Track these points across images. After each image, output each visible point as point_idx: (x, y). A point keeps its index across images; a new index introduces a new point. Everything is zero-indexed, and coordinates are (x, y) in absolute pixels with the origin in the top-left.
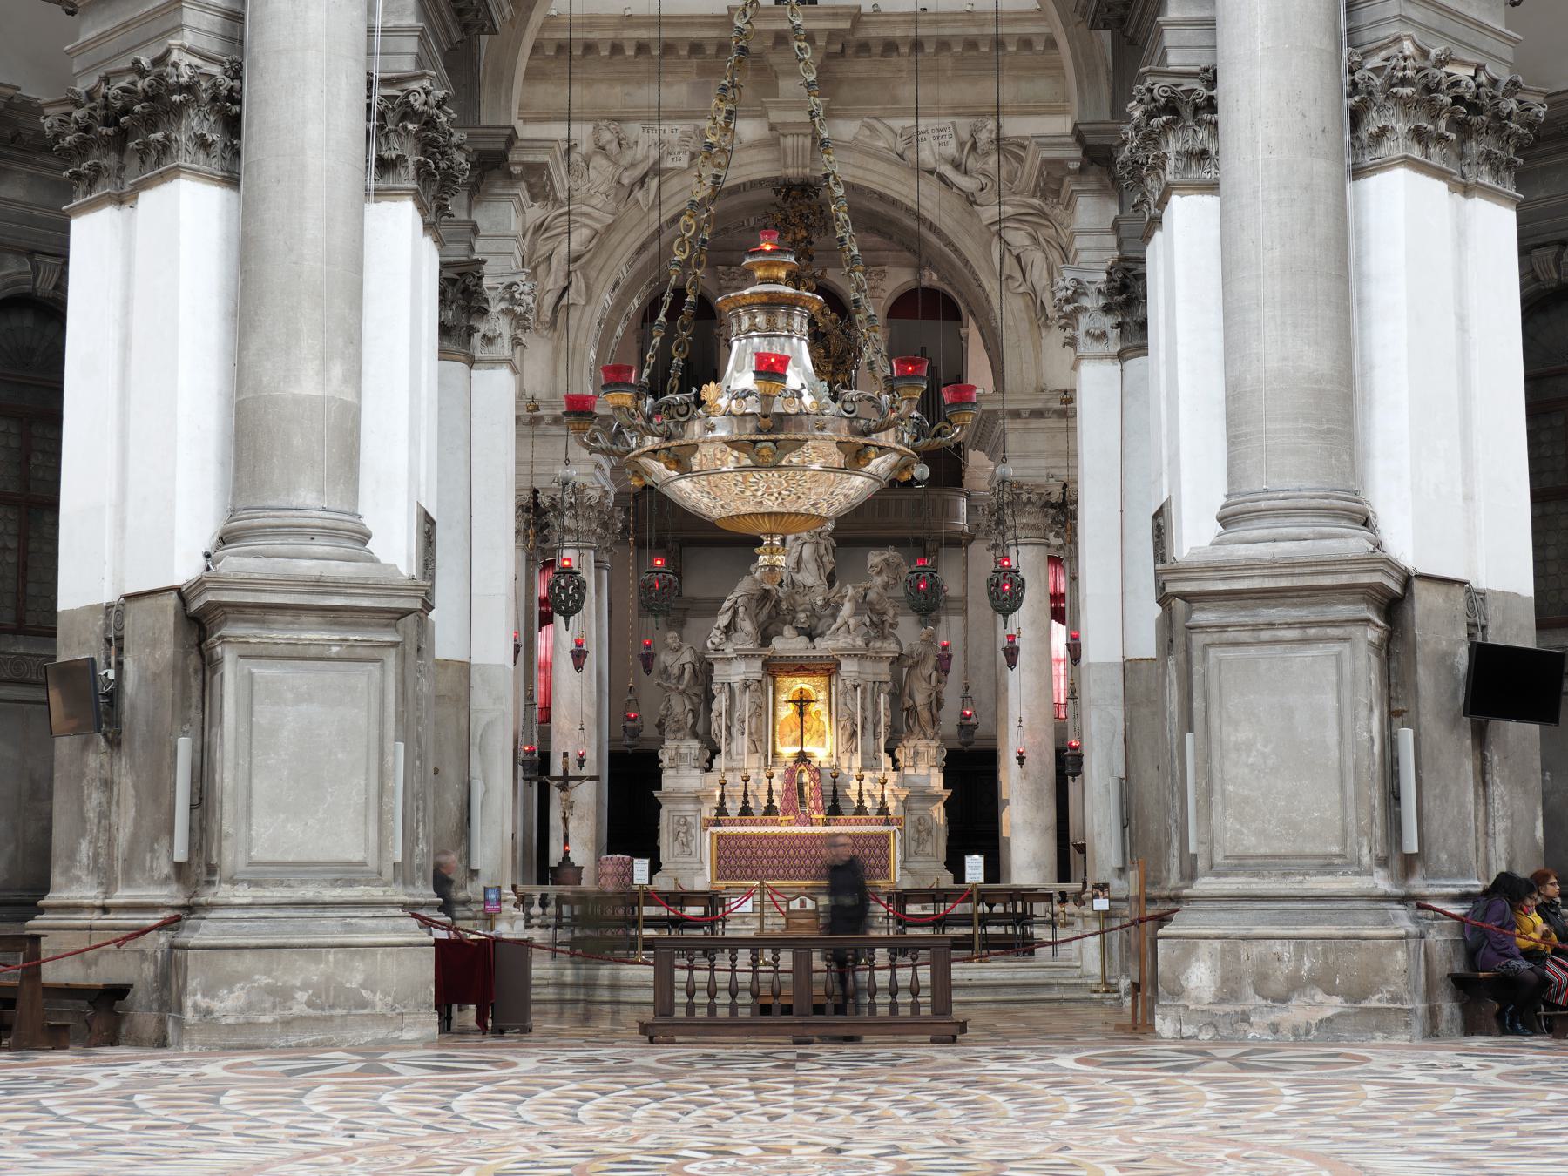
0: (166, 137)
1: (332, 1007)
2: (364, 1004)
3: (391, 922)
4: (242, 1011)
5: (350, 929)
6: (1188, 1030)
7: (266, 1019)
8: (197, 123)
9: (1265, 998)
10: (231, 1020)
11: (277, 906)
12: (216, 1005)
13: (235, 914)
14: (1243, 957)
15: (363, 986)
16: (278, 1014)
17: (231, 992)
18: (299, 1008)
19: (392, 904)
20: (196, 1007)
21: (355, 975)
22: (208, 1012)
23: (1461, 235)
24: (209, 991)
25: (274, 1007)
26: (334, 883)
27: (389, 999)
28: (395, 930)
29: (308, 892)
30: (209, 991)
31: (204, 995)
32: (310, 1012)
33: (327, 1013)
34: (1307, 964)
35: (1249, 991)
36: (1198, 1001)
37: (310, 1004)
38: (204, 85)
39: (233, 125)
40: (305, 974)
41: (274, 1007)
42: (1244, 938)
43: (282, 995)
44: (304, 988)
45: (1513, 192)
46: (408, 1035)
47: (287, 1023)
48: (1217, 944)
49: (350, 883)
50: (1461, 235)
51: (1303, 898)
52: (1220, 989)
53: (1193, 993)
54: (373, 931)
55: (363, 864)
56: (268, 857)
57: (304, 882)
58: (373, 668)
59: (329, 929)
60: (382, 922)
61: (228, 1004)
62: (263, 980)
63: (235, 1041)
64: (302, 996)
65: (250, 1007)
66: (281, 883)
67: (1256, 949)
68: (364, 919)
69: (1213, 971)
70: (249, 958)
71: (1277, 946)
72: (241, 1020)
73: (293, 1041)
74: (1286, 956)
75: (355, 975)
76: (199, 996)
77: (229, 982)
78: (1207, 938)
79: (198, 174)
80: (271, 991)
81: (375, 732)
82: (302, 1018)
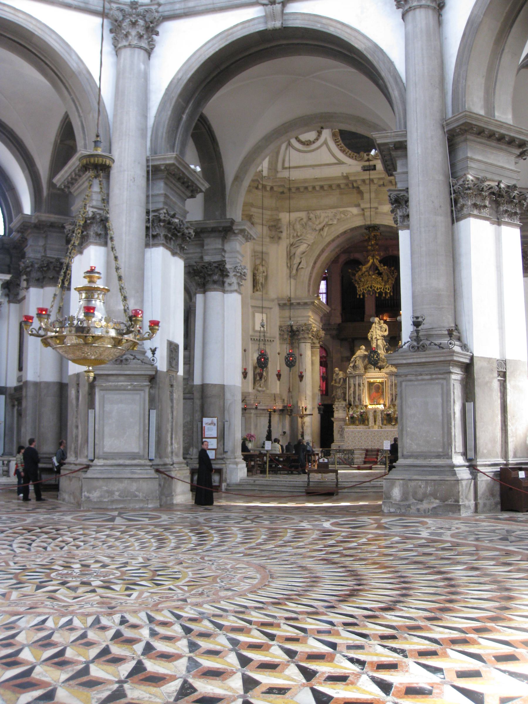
0: (87, 233)
1: (127, 497)
2: (136, 496)
3: (146, 471)
4: (99, 498)
5: (133, 473)
6: (392, 510)
7: (105, 500)
8: (95, 229)
9: (416, 500)
10: (95, 500)
11: (112, 466)
12: (91, 495)
13: (98, 468)
14: (409, 486)
15: (136, 491)
16: (109, 498)
17: (95, 492)
18: (116, 495)
19: (147, 465)
20: (85, 496)
21: (134, 487)
22: (89, 497)
23: (498, 239)
24: (89, 491)
25: (109, 497)
26: (129, 459)
27: (144, 495)
28: (147, 474)
29: (121, 462)
30: (89, 491)
31: (87, 493)
32: (119, 498)
33: (125, 498)
34: (429, 489)
35: (411, 497)
36: (395, 500)
37: (119, 496)
38: (98, 216)
39: (106, 229)
40: (117, 487)
41: (109, 497)
42: (410, 480)
43: (111, 493)
44: (117, 491)
45: (518, 223)
46: (150, 506)
47: (112, 502)
48: (401, 482)
49: (134, 459)
50: (498, 239)
51: (430, 466)
52: (402, 497)
53: (394, 498)
54: (140, 474)
55: (138, 453)
56: (109, 451)
57: (120, 459)
58: (142, 393)
59: (126, 473)
60: (143, 471)
61: (95, 495)
62: (105, 488)
63: (97, 506)
64: (117, 493)
65: (101, 496)
66: (113, 459)
67: (413, 484)
68: (138, 470)
69: (400, 491)
70: (101, 482)
71: (420, 483)
72: (98, 500)
73: (114, 507)
74: (422, 486)
75: (134, 487)
76: (86, 493)
77: (95, 489)
78: (398, 480)
79: (96, 244)
80: (107, 492)
81: (142, 412)
82: (117, 500)
